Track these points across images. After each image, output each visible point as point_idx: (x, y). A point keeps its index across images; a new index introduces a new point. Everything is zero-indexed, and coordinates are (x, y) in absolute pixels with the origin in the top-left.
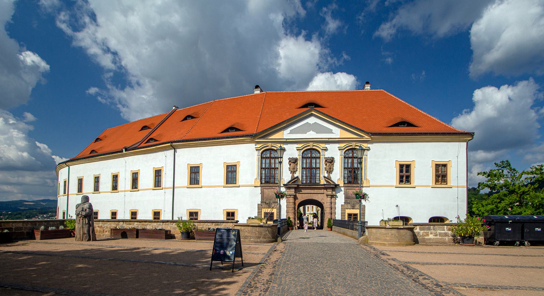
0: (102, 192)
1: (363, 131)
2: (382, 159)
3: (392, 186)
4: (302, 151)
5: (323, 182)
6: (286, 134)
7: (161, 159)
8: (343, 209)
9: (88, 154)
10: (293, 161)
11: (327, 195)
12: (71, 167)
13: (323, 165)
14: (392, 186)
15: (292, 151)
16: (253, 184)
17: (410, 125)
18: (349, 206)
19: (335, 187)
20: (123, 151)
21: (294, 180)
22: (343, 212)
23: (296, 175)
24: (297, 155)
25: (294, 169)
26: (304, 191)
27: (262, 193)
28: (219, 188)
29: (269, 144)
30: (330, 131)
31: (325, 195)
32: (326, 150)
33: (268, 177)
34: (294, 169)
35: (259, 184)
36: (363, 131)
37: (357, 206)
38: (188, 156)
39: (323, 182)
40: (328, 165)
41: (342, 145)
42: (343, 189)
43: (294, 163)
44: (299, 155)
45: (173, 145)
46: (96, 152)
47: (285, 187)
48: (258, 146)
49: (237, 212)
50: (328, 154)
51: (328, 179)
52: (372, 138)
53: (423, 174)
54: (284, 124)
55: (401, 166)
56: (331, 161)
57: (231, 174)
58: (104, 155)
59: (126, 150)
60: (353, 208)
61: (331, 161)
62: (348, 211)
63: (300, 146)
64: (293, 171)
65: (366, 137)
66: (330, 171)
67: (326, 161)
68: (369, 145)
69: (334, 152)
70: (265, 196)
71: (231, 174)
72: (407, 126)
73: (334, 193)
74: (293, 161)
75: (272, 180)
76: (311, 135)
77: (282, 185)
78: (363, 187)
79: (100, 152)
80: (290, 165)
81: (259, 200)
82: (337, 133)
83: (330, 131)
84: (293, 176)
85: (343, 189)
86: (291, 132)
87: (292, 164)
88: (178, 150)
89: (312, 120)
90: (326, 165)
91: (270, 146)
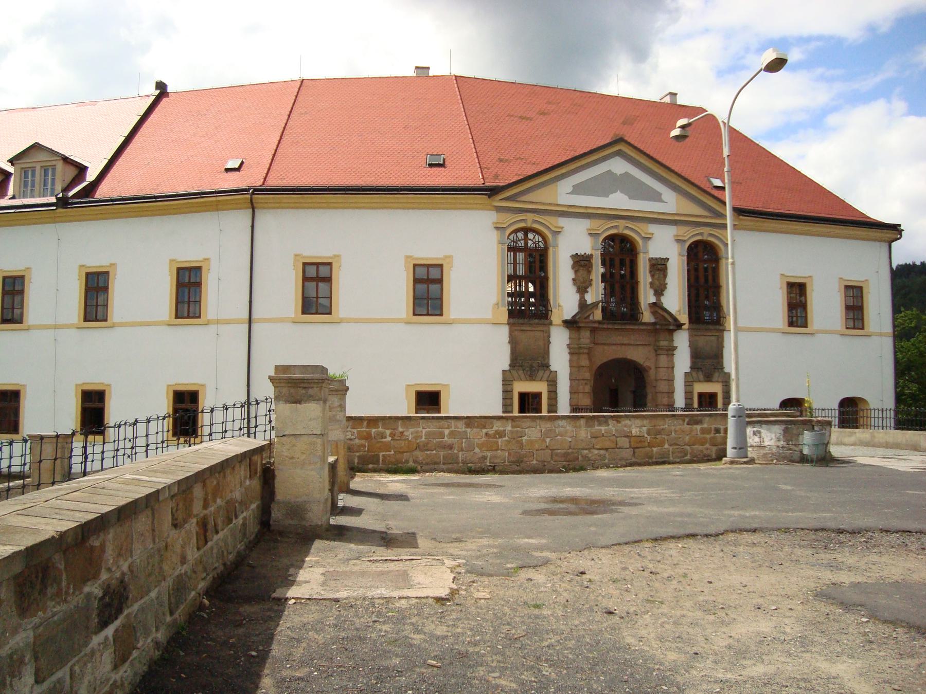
0: (122, 325)
3: (773, 331)
8: (689, 384)
10: (581, 263)
13: (644, 276)
14: (773, 331)
22: (689, 388)
23: (590, 298)
27: (513, 341)
29: (530, 217)
34: (584, 282)
35: (504, 317)
37: (716, 375)
44: (593, 248)
51: (657, 307)
53: (826, 306)
56: (659, 267)
57: (428, 291)
61: (659, 267)
64: (582, 287)
66: (659, 290)
71: (428, 291)
74: (581, 263)
76: (618, 201)
81: (505, 364)
83: (657, 197)
86: (578, 189)
91: (529, 220)
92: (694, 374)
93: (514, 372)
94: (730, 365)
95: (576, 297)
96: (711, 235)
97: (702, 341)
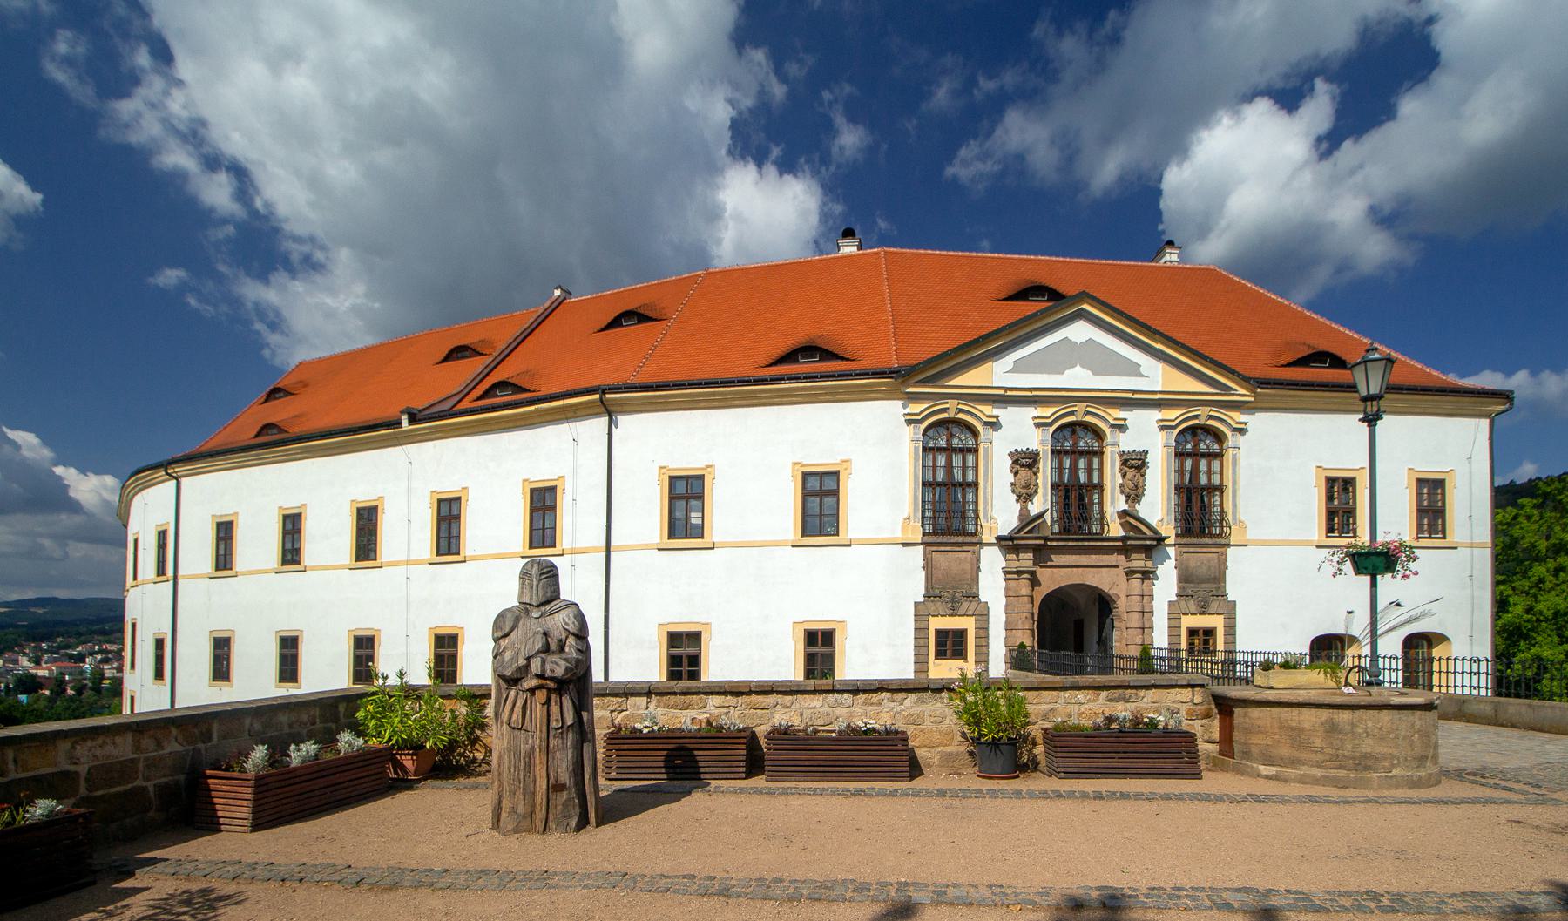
1: (1233, 372)
2: (1282, 459)
4: (1052, 429)
5: (1115, 530)
6: (1000, 373)
7: (560, 450)
9: (247, 435)
10: (1025, 462)
11: (1130, 573)
12: (184, 481)
13: (1112, 476)
15: (1021, 429)
16: (898, 534)
17: (1338, 362)
18: (1192, 606)
19: (1152, 545)
20: (399, 424)
21: (1028, 522)
24: (1037, 441)
25: (1027, 487)
26: (1057, 559)
28: (779, 551)
30: (1134, 370)
31: (1120, 571)
32: (1122, 428)
33: (947, 512)
34: (1027, 487)
36: (1233, 372)
38: (658, 440)
39: (1115, 530)
40: (1129, 476)
41: (1172, 414)
42: (1171, 551)
43: (1030, 466)
45: (607, 400)
46: (282, 430)
47: (1001, 547)
48: (916, 408)
49: (844, 629)
50: (1128, 442)
52: (1256, 395)
54: (998, 339)
55: (1331, 482)
56: (1135, 463)
58: (322, 436)
59: (413, 419)
60: (1203, 610)
61: (1135, 463)
62: (1188, 622)
63: (1047, 412)
64: (1025, 494)
65: (1241, 392)
66: (1134, 494)
67: (1124, 463)
68: (1242, 418)
69: (1146, 434)
70: (938, 574)
72: (1331, 366)
73: (1149, 564)
74: (1025, 462)
75: (956, 522)
76: (1078, 378)
77: (988, 537)
78: (1229, 545)
79: (296, 430)
80: (1016, 474)
82: (1155, 376)
83: (1134, 370)
84: (1024, 513)
85: (1171, 551)
86: (1018, 367)
87: (1023, 473)
88: (621, 419)
89: (1079, 332)
90: (1124, 476)
92: (1183, 603)
93: (930, 605)
94: (1232, 591)
95: (1018, 506)
96: (1211, 417)
97: (1200, 561)
